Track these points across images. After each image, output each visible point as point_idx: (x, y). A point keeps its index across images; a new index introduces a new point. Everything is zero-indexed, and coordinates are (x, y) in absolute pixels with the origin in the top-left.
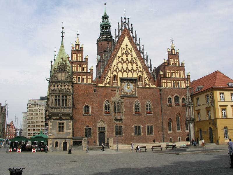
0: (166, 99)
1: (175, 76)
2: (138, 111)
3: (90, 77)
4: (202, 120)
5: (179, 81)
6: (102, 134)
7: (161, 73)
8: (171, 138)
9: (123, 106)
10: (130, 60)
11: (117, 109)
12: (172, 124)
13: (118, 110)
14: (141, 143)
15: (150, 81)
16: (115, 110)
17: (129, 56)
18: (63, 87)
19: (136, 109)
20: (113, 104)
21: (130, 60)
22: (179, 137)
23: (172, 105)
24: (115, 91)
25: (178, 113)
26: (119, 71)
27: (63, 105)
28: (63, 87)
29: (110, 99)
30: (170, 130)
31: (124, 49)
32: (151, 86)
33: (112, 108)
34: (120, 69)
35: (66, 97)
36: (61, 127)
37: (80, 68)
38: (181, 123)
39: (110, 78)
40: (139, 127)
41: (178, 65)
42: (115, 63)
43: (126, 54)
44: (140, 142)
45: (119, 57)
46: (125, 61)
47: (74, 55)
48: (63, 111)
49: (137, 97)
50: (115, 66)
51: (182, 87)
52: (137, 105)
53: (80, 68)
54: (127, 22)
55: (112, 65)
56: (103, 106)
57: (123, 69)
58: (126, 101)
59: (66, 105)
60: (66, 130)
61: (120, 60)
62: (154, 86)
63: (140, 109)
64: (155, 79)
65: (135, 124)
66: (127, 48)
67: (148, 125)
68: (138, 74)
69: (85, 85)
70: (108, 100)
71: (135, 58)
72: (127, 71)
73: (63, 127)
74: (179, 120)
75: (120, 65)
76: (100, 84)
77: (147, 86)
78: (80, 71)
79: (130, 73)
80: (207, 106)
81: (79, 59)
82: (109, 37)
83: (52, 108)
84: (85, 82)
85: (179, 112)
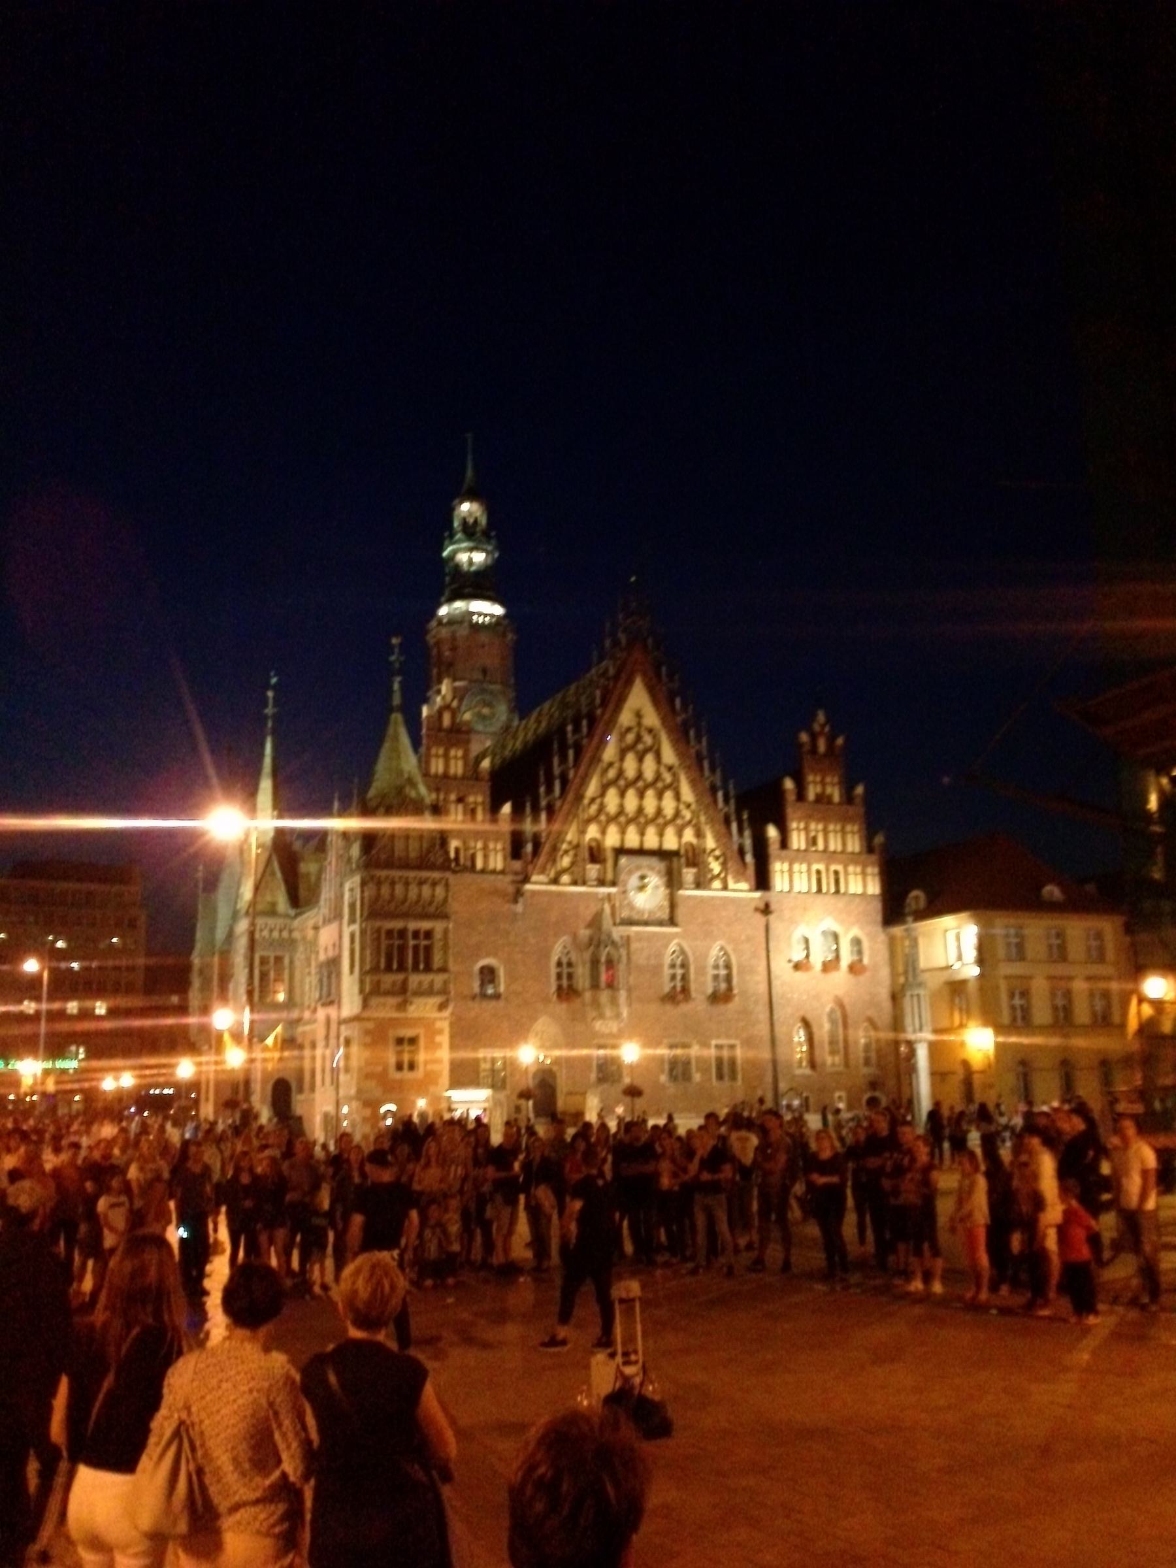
7: (772, 832)
10: (649, 774)
15: (724, 865)
17: (649, 761)
20: (587, 955)
26: (612, 819)
28: (413, 892)
31: (629, 729)
42: (592, 789)
45: (611, 765)
47: (433, 751)
52: (679, 962)
66: (639, 724)
71: (670, 768)
79: (651, 832)
84: (479, 864)
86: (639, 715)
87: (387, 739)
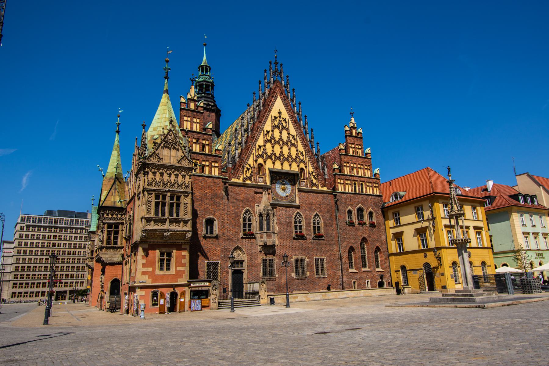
0: (345, 211)
1: (357, 173)
2: (300, 232)
3: (217, 165)
4: (405, 250)
5: (364, 183)
6: (238, 274)
7: (336, 166)
8: (354, 282)
9: (275, 222)
10: (285, 139)
11: (265, 226)
12: (355, 256)
13: (268, 229)
14: (307, 292)
16: (261, 228)
17: (285, 133)
18: (173, 178)
19: (296, 227)
20: (257, 216)
21: (285, 139)
22: (367, 280)
23: (353, 223)
24: (262, 193)
25: (364, 237)
27: (171, 214)
28: (173, 178)
29: (254, 207)
30: (351, 267)
31: (276, 118)
32: (320, 188)
33: (255, 224)
34: (269, 154)
35: (178, 198)
36: (165, 260)
37: (198, 146)
38: (368, 254)
39: (251, 168)
40: (303, 260)
41: (361, 155)
42: (260, 141)
43: (278, 128)
44: (305, 290)
46: (277, 139)
48: (172, 228)
49: (298, 207)
50: (260, 147)
51: (368, 193)
53: (198, 146)
54: (279, 71)
55: (255, 145)
56: (239, 219)
57: (275, 155)
58: (280, 212)
59: (178, 215)
60: (176, 267)
61: (269, 138)
62: (325, 189)
63: (304, 228)
64: (326, 177)
65: (295, 255)
66: (280, 117)
67: (318, 257)
68: (298, 166)
69: (206, 179)
70: (250, 209)
71: (293, 137)
72: (281, 158)
73: (169, 261)
74: (364, 249)
75: (269, 146)
76: (234, 178)
77: (314, 188)
78: (198, 151)
80: (419, 226)
81: (197, 128)
82: (212, 104)
83: (148, 220)
85: (365, 236)
86: (280, 113)
87: (161, 104)
